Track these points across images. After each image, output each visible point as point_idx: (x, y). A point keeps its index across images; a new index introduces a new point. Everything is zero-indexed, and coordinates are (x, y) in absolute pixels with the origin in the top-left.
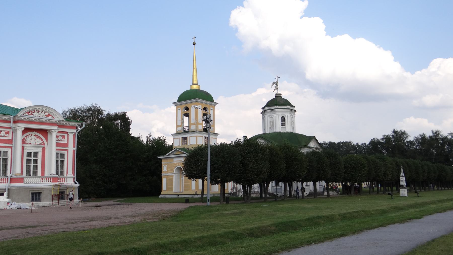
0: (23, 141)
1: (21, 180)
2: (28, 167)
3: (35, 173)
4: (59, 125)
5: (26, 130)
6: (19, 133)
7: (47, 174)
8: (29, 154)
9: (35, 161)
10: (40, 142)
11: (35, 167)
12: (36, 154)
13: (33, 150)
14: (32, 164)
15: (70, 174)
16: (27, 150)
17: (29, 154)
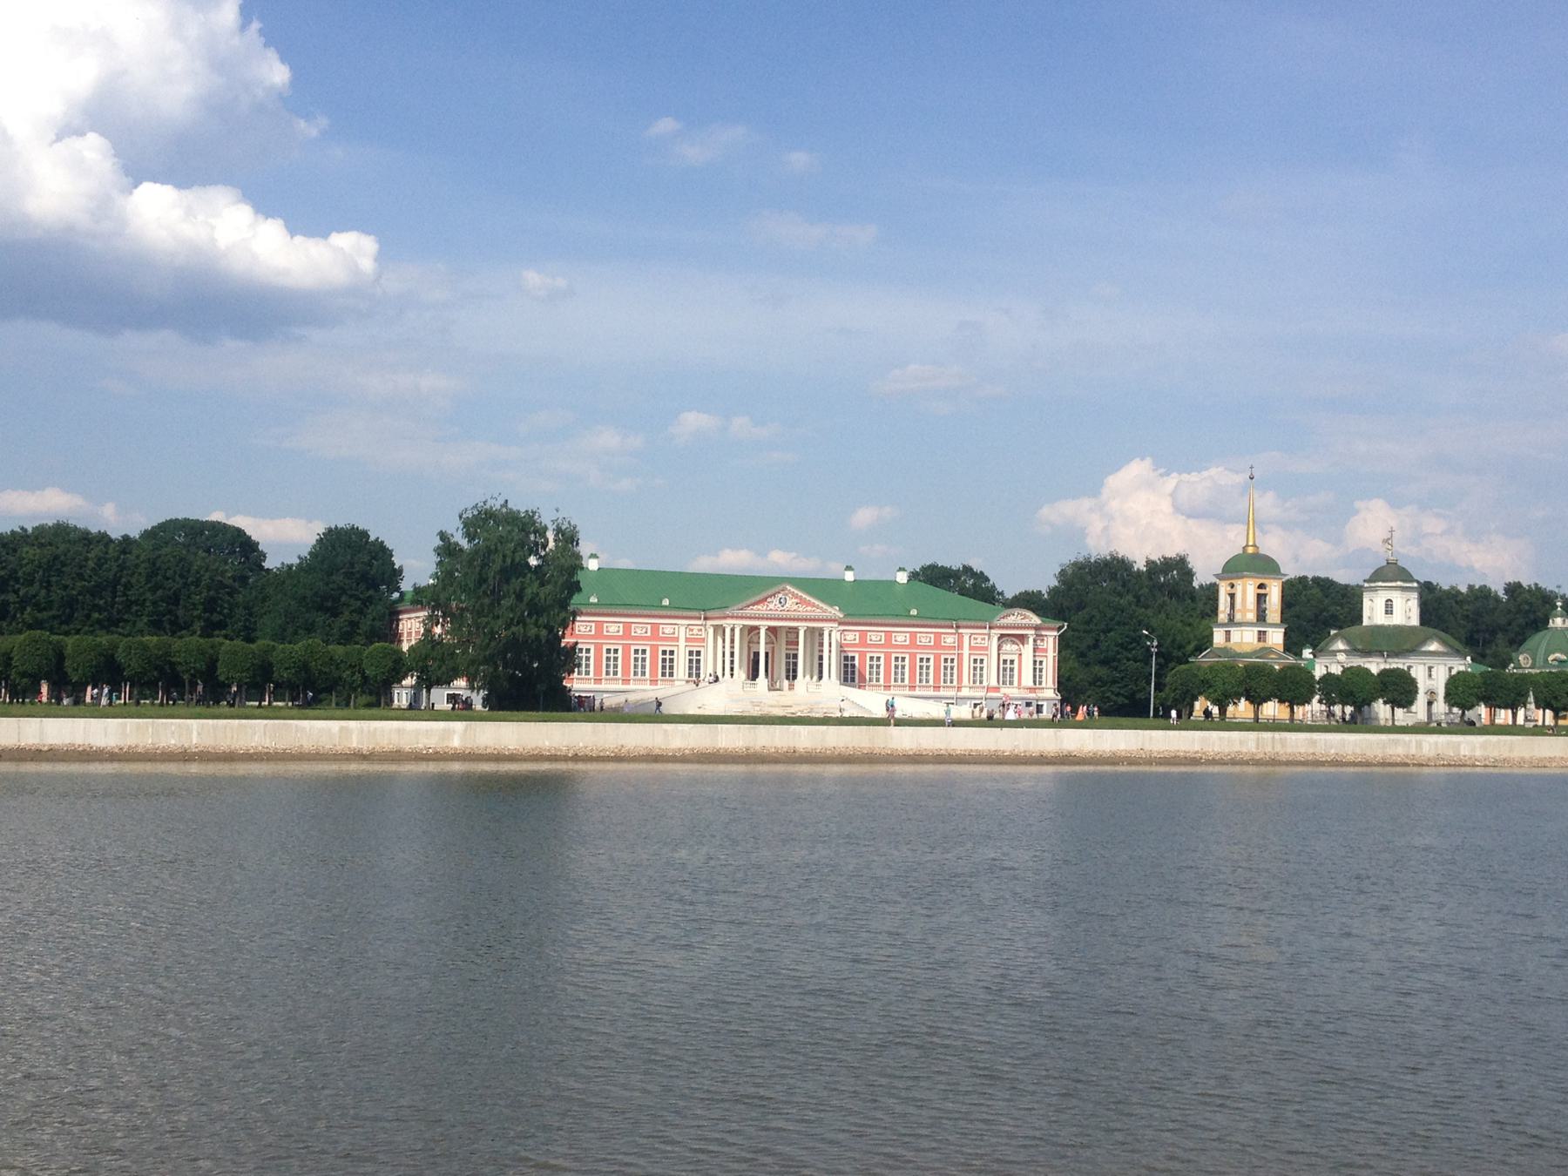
0: (999, 648)
1: (997, 689)
3: (1011, 683)
4: (1037, 628)
5: (1002, 636)
6: (995, 640)
7: (1024, 683)
9: (1012, 670)
10: (1015, 647)
11: (1012, 676)
12: (1012, 662)
13: (1009, 658)
14: (1007, 670)
15: (1050, 684)
16: (1002, 657)
17: (1005, 662)
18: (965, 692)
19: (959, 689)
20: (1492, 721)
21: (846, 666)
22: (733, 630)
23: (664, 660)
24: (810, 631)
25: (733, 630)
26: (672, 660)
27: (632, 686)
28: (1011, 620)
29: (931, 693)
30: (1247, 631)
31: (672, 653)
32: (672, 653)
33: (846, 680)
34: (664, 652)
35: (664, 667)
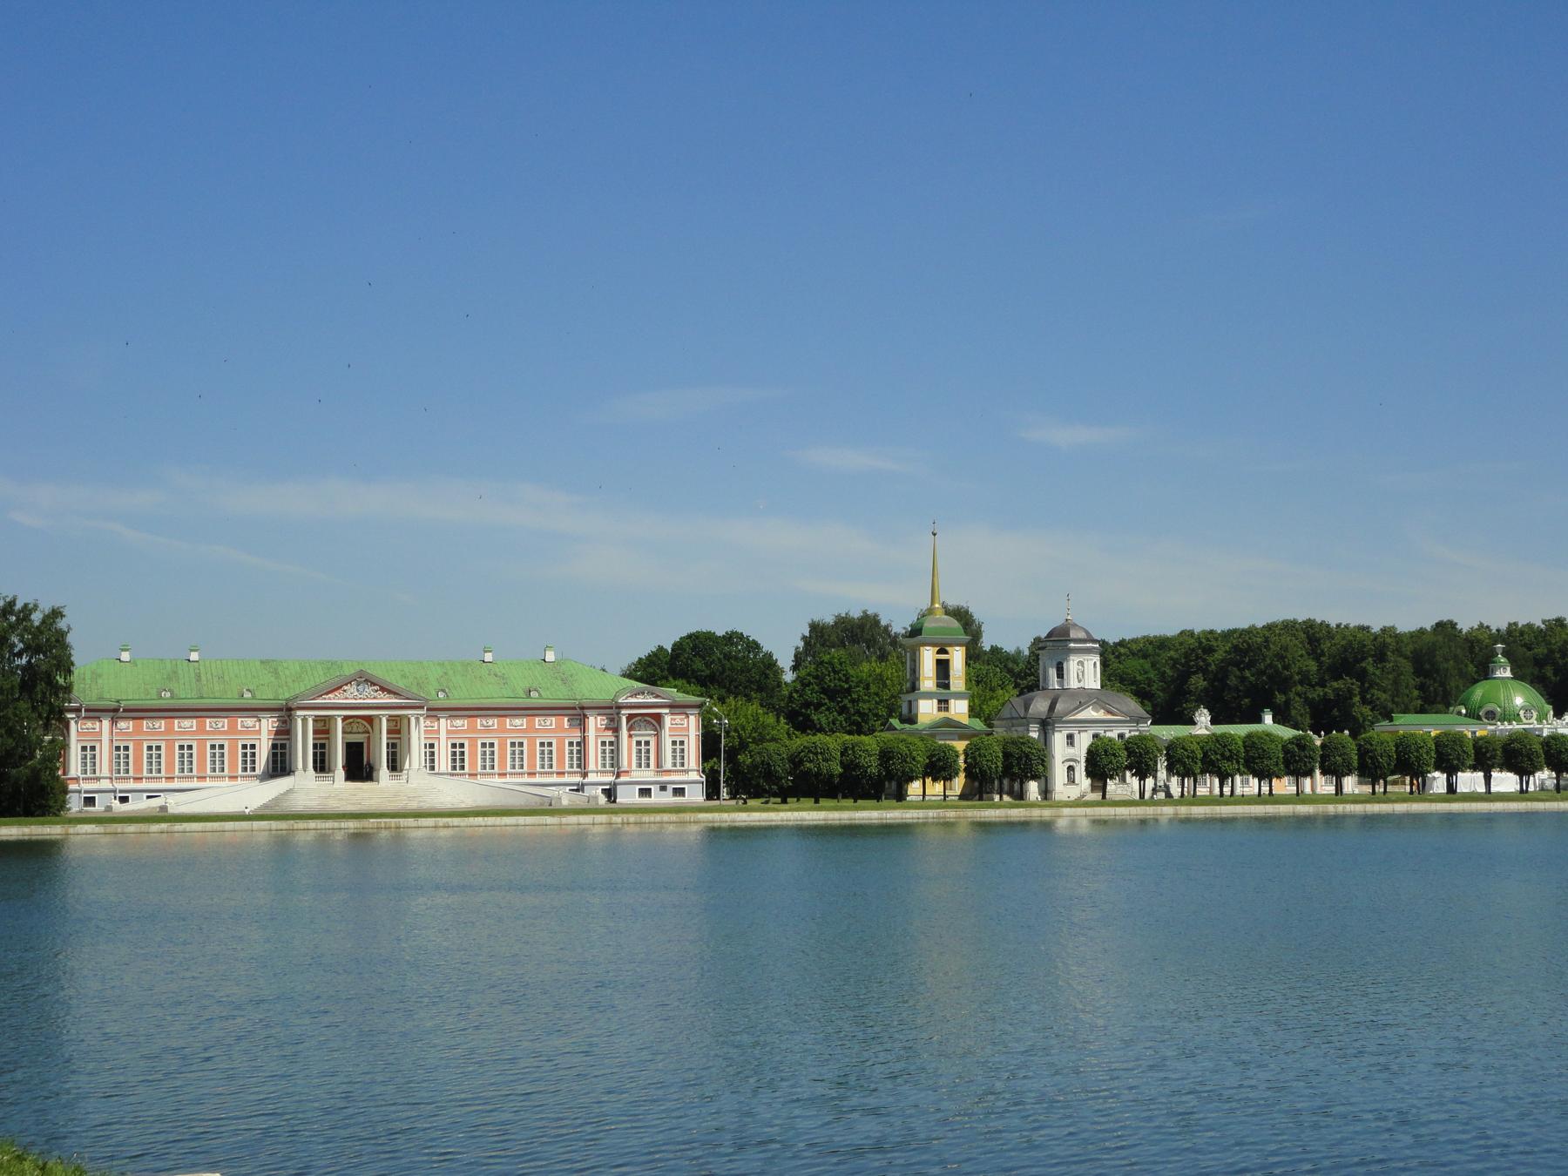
2: (640, 758)
5: (630, 717)
6: (624, 719)
8: (639, 743)
18: (592, 778)
19: (585, 775)
20: (1451, 789)
21: (454, 754)
22: (305, 720)
23: (245, 755)
24: (391, 719)
25: (305, 720)
26: (253, 755)
27: (208, 783)
28: (640, 700)
29: (554, 779)
30: (941, 705)
31: (253, 746)
32: (253, 746)
33: (454, 768)
34: (244, 747)
35: (245, 762)
